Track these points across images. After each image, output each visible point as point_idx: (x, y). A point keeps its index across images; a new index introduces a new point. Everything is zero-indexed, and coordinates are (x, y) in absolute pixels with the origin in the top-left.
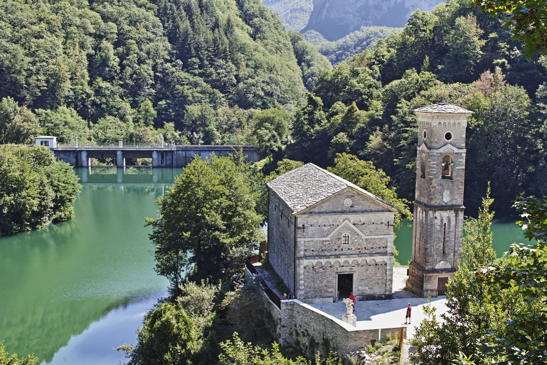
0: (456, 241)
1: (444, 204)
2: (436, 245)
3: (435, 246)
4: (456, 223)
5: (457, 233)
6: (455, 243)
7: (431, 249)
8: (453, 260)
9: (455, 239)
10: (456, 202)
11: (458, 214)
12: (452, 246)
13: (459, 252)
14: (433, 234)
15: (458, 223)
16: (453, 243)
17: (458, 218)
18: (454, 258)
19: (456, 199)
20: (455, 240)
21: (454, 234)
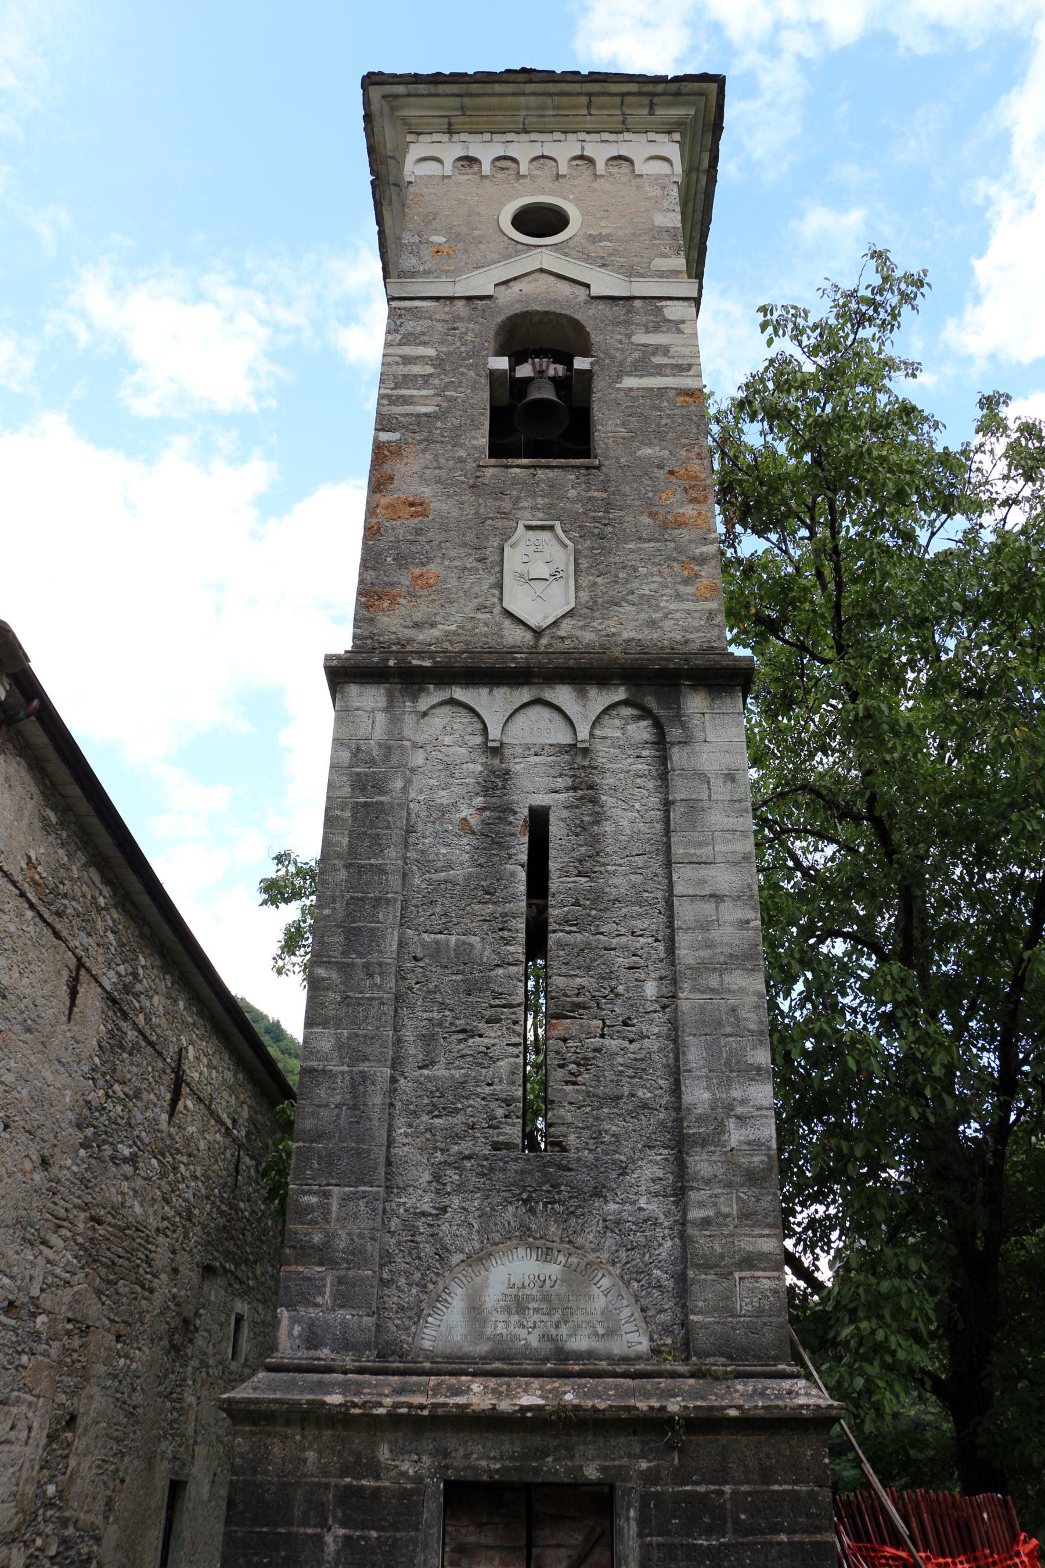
0: (689, 1001)
1: (515, 636)
2: (428, 1039)
3: (413, 1051)
4: (667, 805)
5: (686, 912)
6: (674, 1024)
7: (360, 1082)
8: (667, 1247)
9: (672, 980)
10: (652, 624)
11: (679, 718)
12: (639, 1069)
13: (735, 1135)
14: (388, 917)
15: (694, 807)
16: (655, 1026)
17: (678, 756)
18: (682, 1228)
19: (645, 599)
20: (669, 1001)
21: (654, 922)
